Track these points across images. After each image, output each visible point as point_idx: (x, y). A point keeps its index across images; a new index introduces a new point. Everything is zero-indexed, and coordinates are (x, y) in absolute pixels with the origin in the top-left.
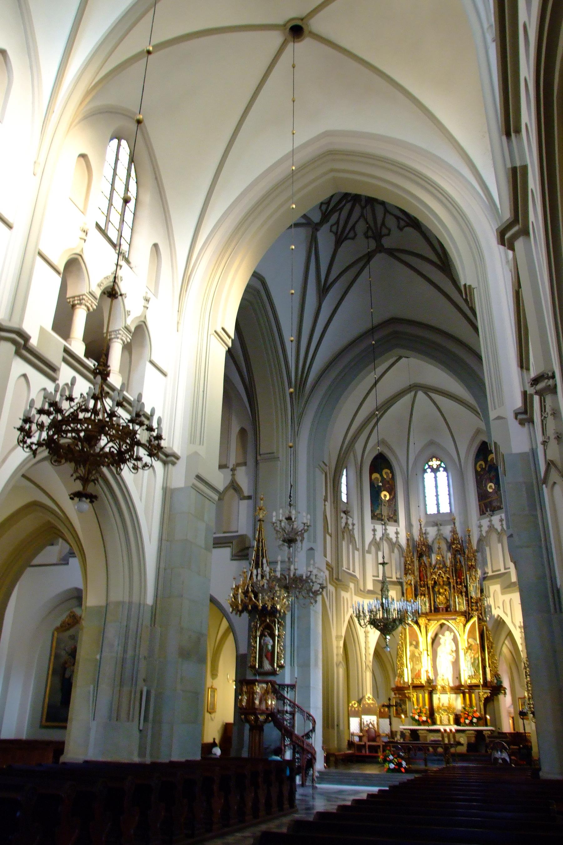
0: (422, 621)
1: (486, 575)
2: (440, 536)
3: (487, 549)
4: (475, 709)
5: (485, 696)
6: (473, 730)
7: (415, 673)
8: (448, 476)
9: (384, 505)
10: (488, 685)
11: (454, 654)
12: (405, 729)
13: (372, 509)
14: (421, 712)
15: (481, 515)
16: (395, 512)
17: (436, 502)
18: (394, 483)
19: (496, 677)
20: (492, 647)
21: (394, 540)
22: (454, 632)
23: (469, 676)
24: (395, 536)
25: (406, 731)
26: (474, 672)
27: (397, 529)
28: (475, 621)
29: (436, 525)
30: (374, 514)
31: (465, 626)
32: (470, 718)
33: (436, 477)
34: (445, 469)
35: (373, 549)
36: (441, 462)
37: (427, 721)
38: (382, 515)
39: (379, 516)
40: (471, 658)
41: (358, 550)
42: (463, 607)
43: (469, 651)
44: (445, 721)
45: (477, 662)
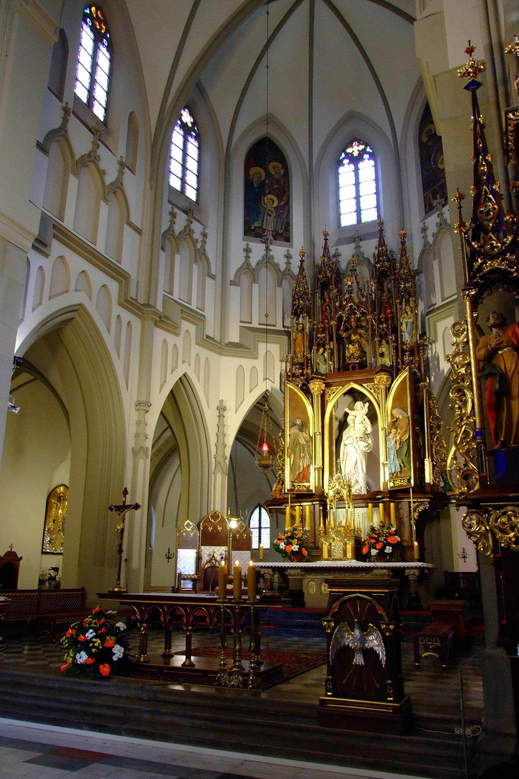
0: (316, 387)
1: (431, 308)
2: (358, 256)
3: (435, 263)
4: (393, 529)
5: (421, 508)
6: (385, 568)
7: (298, 472)
8: (375, 166)
9: (269, 215)
10: (428, 489)
11: (370, 441)
12: (262, 567)
13: (247, 219)
14: (292, 537)
15: (426, 212)
16: (287, 227)
17: (354, 208)
18: (288, 182)
19: (443, 477)
20: (439, 427)
21: (283, 267)
22: (371, 403)
23: (393, 474)
24: (285, 260)
25: (266, 571)
26: (401, 466)
27: (288, 250)
28: (406, 377)
29: (354, 241)
30: (250, 227)
31: (388, 390)
32: (379, 546)
33: (356, 171)
34: (372, 156)
35: (245, 279)
36: (366, 145)
37: (299, 552)
38: (264, 231)
39: (260, 231)
40: (396, 442)
41: (213, 277)
42: (388, 360)
43: (393, 431)
44: (338, 553)
45: (405, 448)
